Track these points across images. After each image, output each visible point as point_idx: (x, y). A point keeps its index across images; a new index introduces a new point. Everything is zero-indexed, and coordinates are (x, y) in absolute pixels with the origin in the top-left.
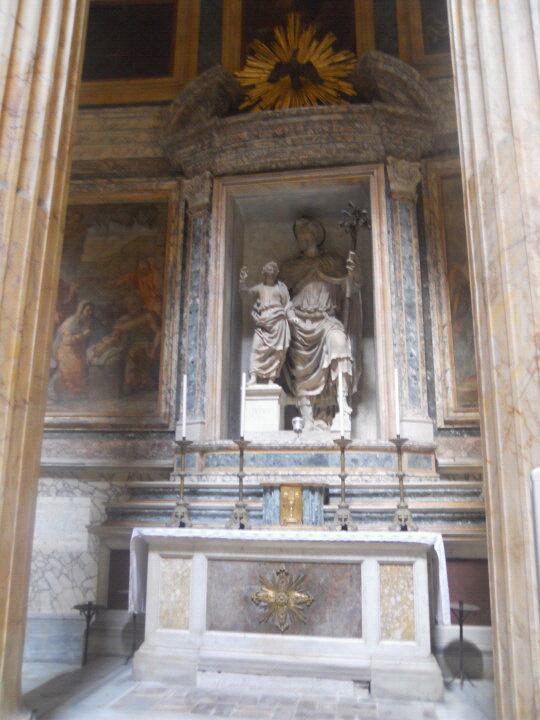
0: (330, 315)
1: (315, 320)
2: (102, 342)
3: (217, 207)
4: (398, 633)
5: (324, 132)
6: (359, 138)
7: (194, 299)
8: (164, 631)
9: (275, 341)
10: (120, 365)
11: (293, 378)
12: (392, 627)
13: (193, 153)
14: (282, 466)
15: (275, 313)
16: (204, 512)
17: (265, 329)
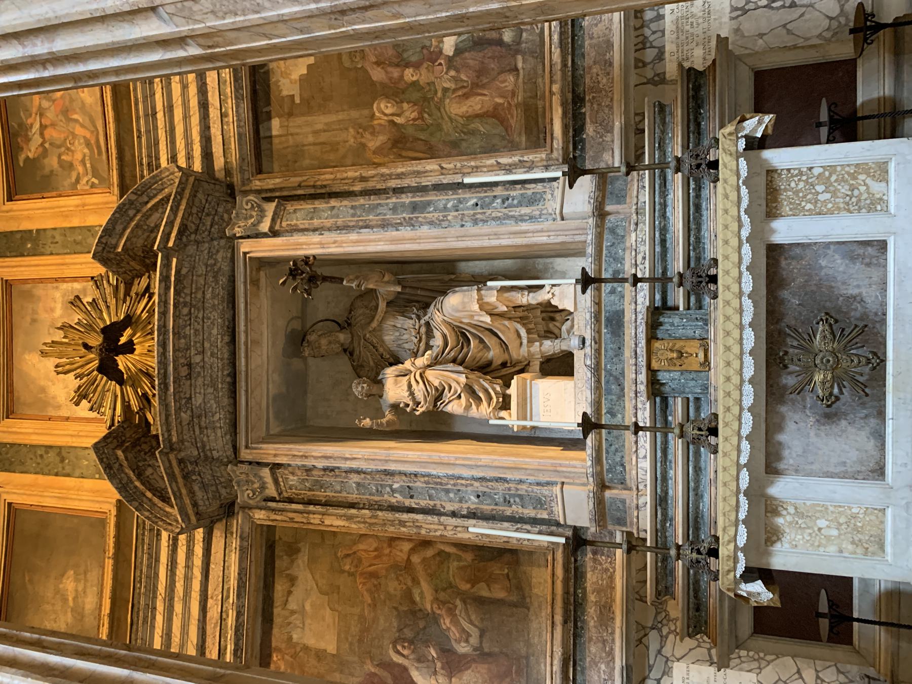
0: (425, 315)
1: (430, 334)
2: (449, 629)
3: (275, 455)
4: (877, 187)
5: (190, 313)
6: (201, 269)
7: (393, 491)
8: (889, 549)
9: (454, 385)
10: (481, 602)
11: (504, 365)
12: (865, 196)
13: (204, 487)
14: (623, 374)
15: (417, 382)
16: (692, 484)
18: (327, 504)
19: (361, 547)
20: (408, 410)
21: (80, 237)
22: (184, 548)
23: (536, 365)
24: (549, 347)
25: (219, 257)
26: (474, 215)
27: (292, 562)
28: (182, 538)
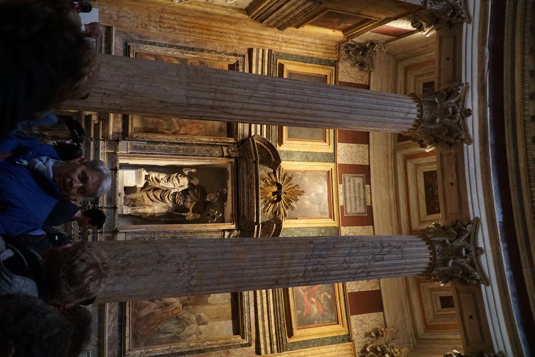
1: (174, 200)
7: (183, 150)
18: (208, 145)
19: (197, 132)
20: (180, 175)
21: (302, 233)
22: (258, 130)
23: (138, 190)
24: (133, 196)
25: (243, 224)
26: (154, 235)
27: (221, 126)
28: (259, 133)
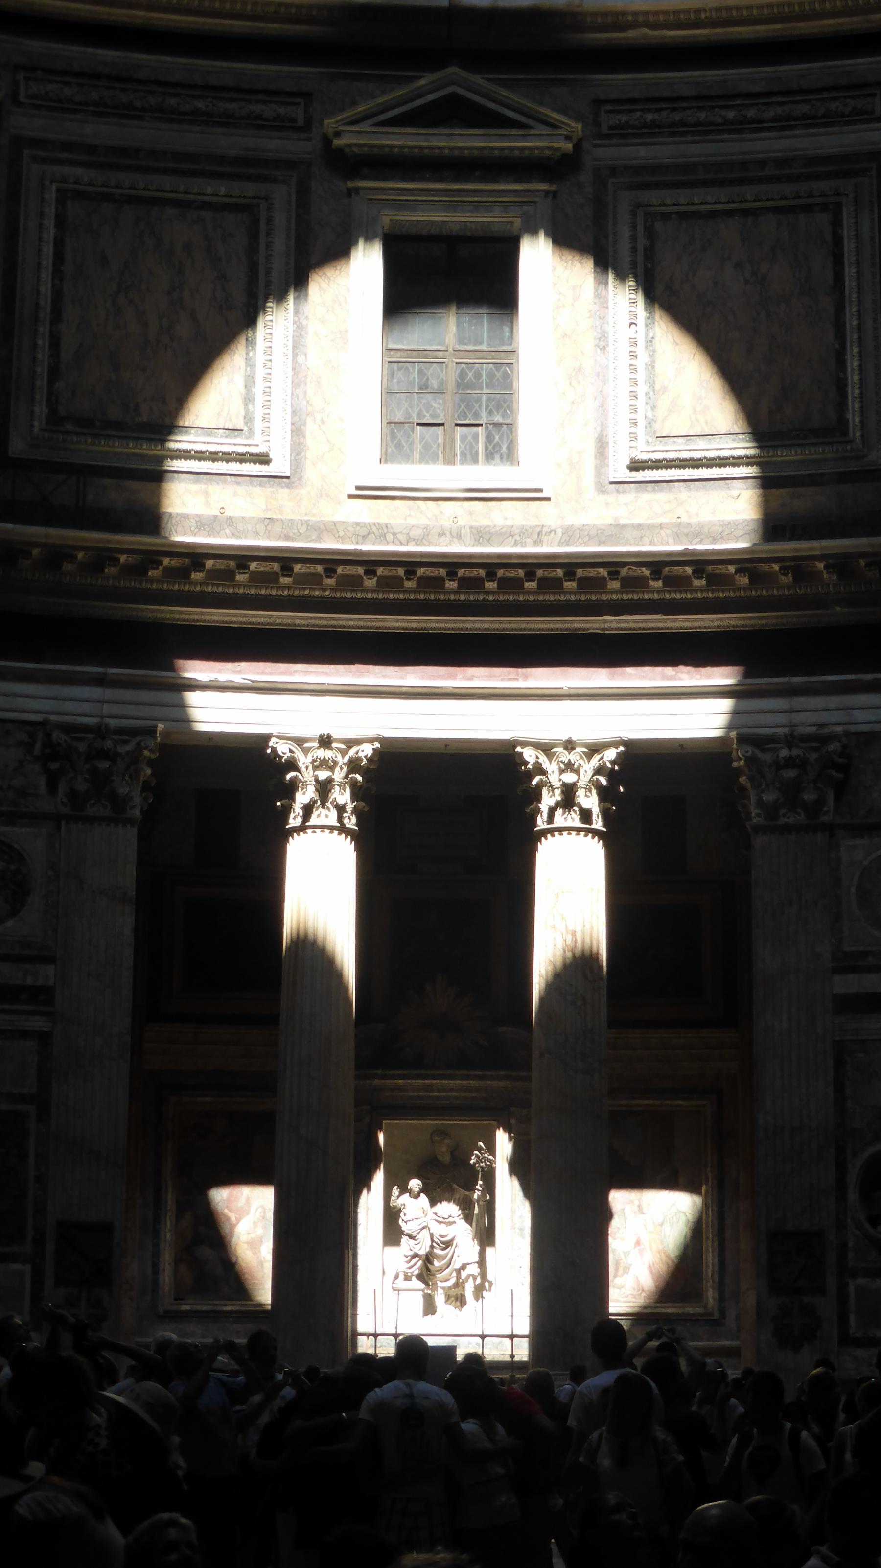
9: (418, 1247)
17: (411, 1237)
